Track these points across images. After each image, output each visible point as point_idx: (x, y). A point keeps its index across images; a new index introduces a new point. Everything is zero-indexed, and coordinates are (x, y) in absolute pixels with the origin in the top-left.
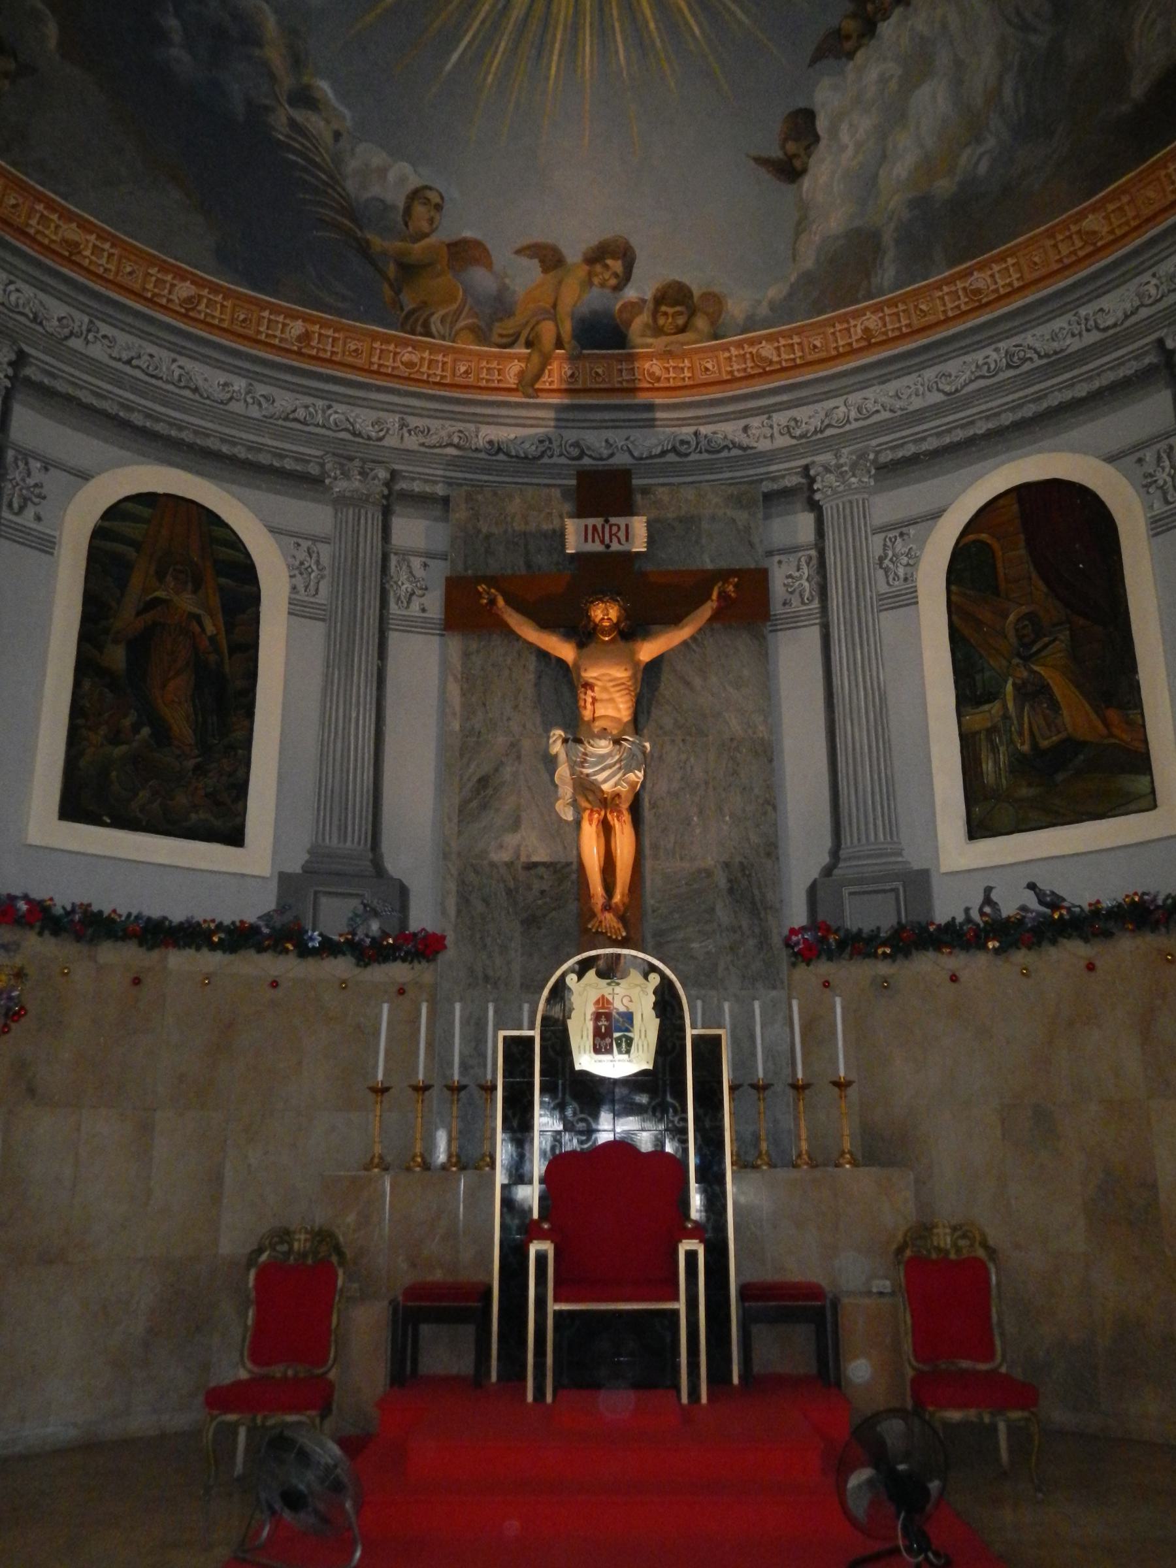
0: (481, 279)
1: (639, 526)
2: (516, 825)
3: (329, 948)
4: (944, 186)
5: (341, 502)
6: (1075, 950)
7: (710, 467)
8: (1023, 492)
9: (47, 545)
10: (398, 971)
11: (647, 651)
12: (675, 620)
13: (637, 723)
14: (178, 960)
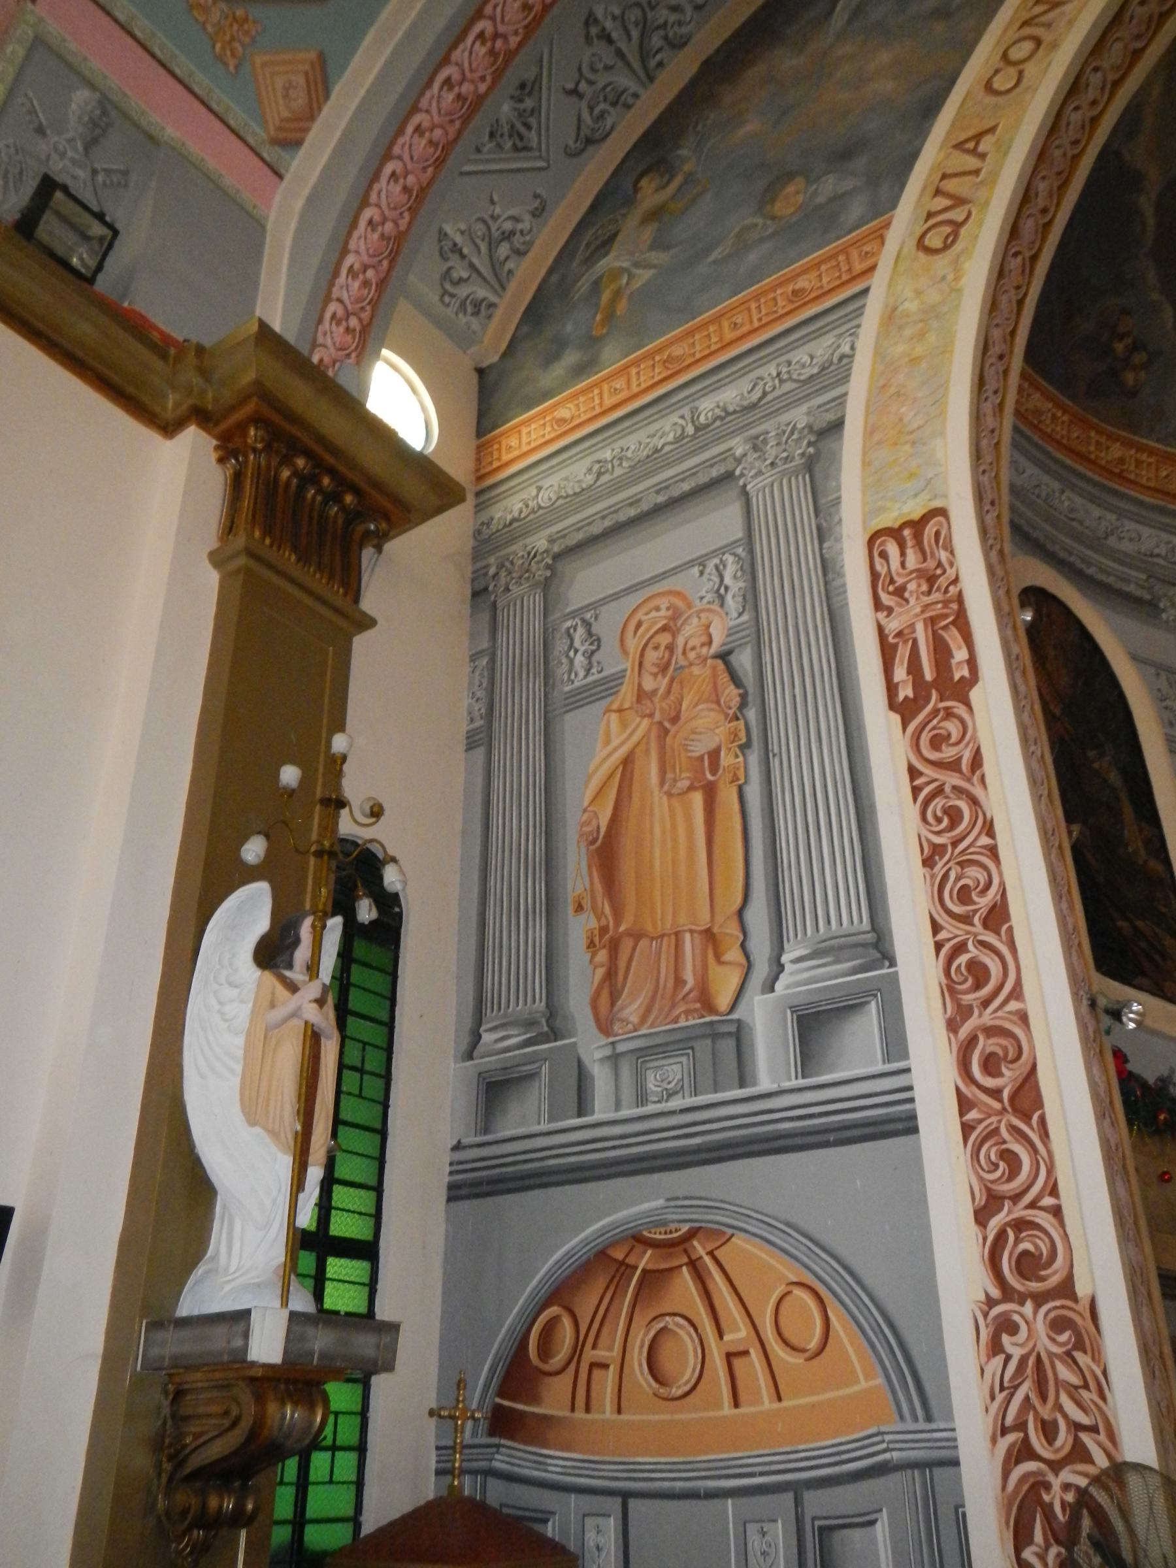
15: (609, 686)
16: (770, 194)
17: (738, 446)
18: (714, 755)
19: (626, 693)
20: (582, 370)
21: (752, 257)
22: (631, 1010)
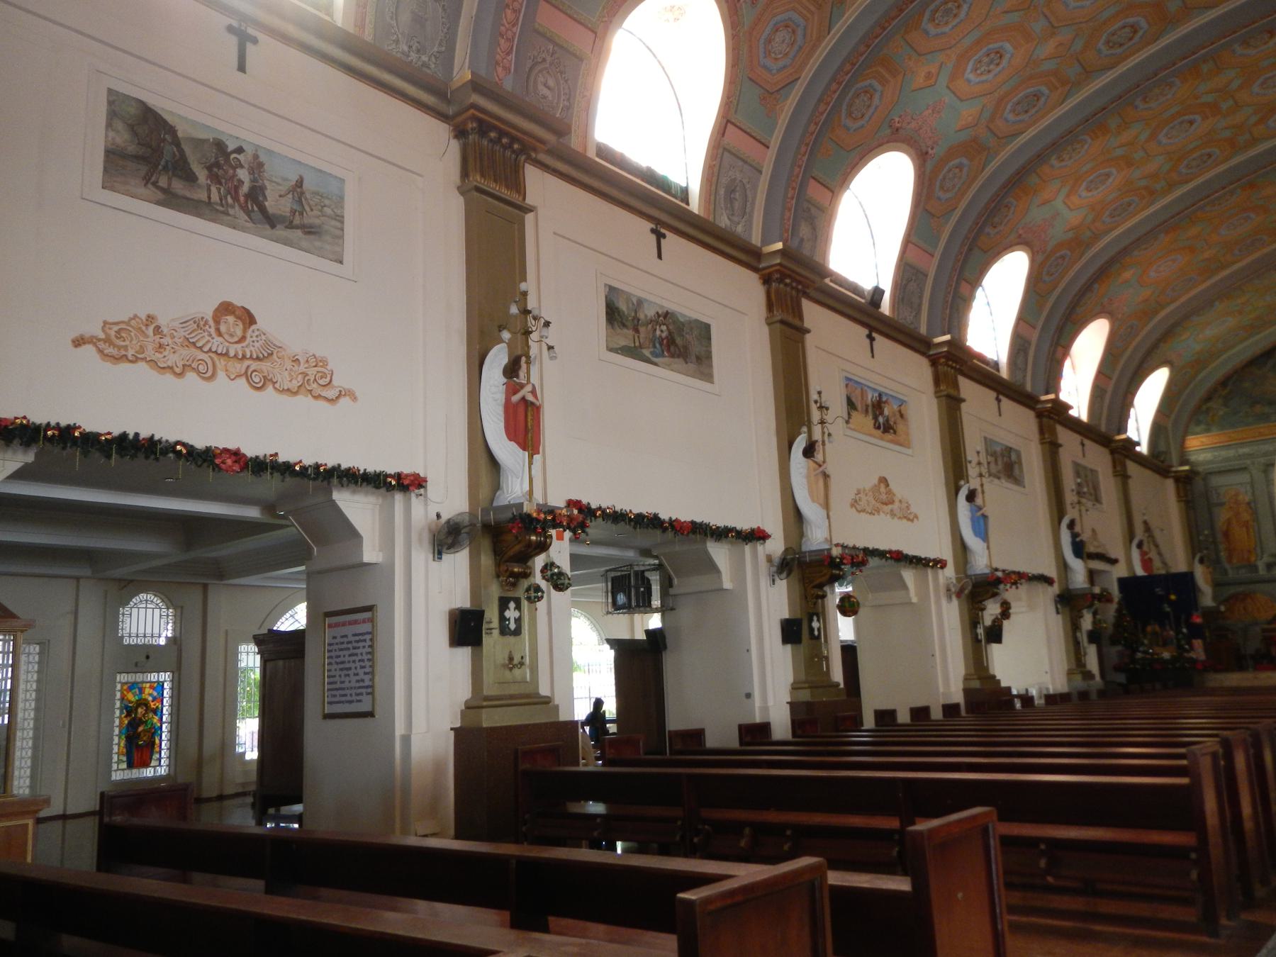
15: (1222, 504)
17: (1248, 462)
18: (1248, 522)
20: (1208, 430)
22: (1235, 561)
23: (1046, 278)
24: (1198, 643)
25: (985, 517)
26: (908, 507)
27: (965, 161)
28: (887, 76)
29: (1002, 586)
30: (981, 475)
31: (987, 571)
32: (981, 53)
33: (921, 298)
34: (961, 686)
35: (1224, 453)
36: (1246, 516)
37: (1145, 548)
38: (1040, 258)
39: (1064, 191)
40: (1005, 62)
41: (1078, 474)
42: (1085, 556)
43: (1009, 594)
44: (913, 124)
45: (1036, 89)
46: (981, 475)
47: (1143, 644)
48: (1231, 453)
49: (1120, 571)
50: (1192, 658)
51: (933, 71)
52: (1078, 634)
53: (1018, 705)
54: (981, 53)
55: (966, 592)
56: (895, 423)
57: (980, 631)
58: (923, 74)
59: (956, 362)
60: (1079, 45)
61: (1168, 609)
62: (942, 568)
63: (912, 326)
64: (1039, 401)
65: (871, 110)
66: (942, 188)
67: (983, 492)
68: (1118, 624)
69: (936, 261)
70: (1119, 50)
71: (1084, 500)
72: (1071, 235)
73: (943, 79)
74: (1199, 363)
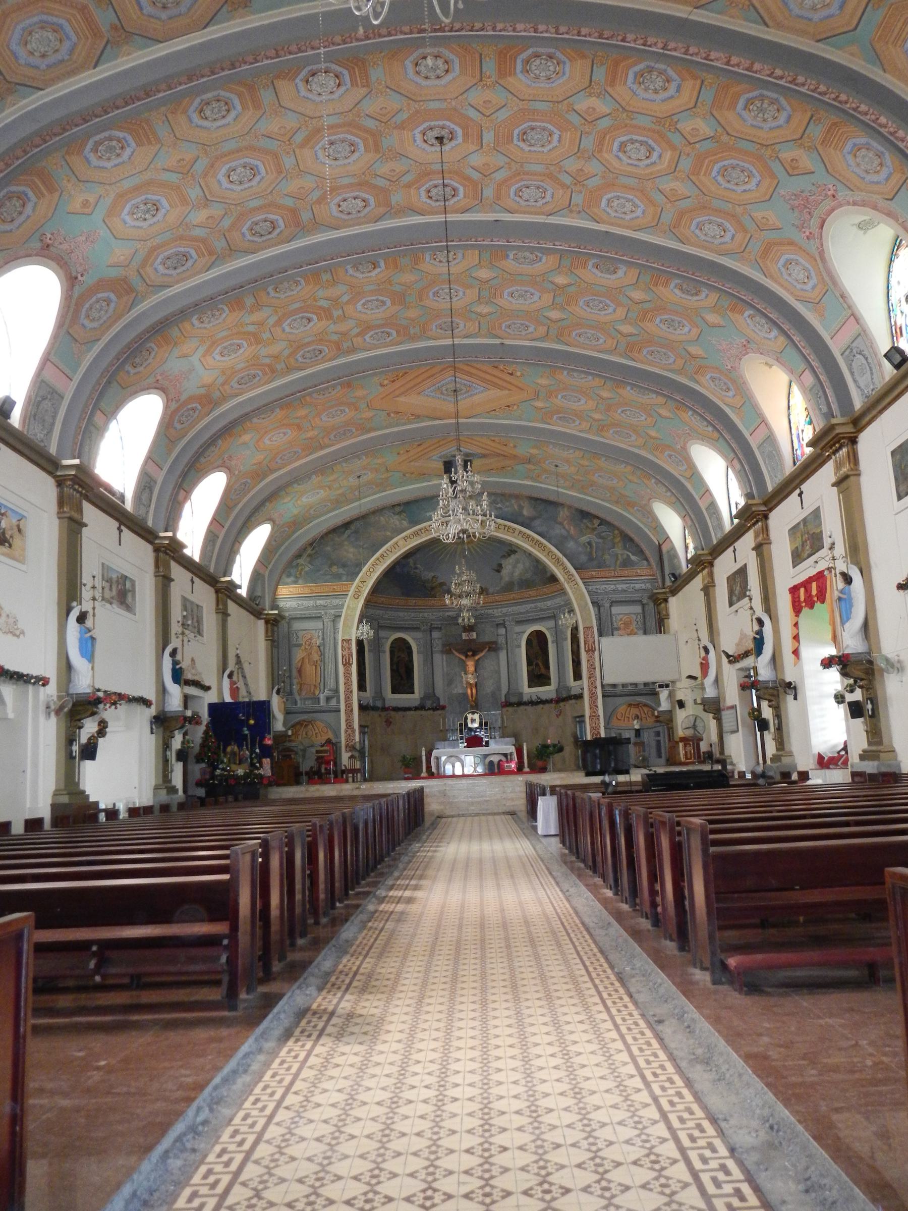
0: (445, 587)
1: (475, 634)
2: (456, 687)
3: (429, 709)
4: (524, 578)
5: (424, 631)
6: (541, 706)
7: (486, 618)
8: (537, 631)
9: (384, 652)
10: (439, 712)
11: (477, 658)
12: (482, 651)
13: (476, 670)
14: (408, 713)
15: (299, 645)
16: (330, 566)
19: (303, 648)
20: (296, 582)
21: (328, 577)
22: (304, 693)
23: (178, 426)
24: (266, 762)
25: (93, 639)
26: (15, 623)
27: (112, 296)
28: (45, 192)
29: (101, 706)
30: (94, 599)
31: (89, 691)
32: (139, 200)
33: (54, 417)
34: (50, 801)
35: (307, 603)
36: (316, 657)
37: (235, 678)
38: (174, 405)
39: (201, 351)
40: (160, 215)
41: (185, 608)
42: (182, 682)
43: (108, 713)
44: (65, 246)
45: (187, 249)
46: (94, 599)
47: (222, 762)
48: (311, 603)
49: (212, 697)
50: (260, 774)
51: (91, 200)
52: (168, 753)
53: (102, 817)
54: (139, 200)
55: (66, 710)
56: (11, 537)
57: (75, 748)
58: (81, 200)
59: (80, 486)
60: (226, 223)
61: (247, 732)
62: (44, 685)
63: (42, 444)
64: (157, 537)
65: (22, 218)
66: (88, 316)
67: (94, 615)
68: (203, 745)
69: (73, 385)
70: (259, 240)
71: (187, 632)
72: (202, 391)
73: (99, 214)
74: (296, 524)
